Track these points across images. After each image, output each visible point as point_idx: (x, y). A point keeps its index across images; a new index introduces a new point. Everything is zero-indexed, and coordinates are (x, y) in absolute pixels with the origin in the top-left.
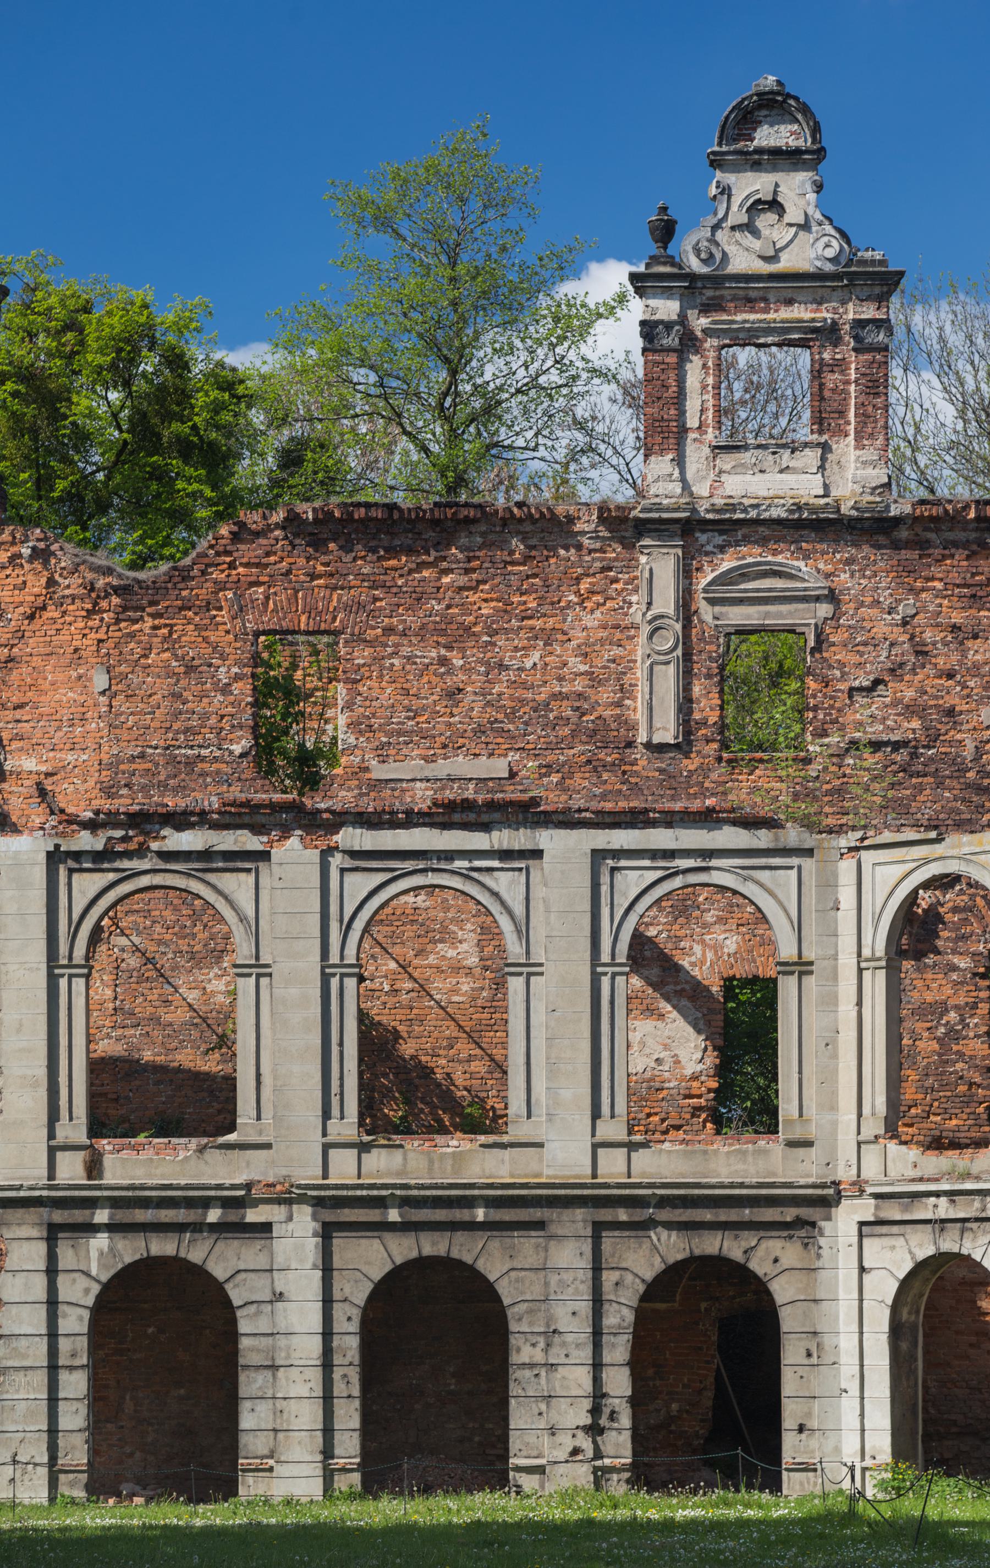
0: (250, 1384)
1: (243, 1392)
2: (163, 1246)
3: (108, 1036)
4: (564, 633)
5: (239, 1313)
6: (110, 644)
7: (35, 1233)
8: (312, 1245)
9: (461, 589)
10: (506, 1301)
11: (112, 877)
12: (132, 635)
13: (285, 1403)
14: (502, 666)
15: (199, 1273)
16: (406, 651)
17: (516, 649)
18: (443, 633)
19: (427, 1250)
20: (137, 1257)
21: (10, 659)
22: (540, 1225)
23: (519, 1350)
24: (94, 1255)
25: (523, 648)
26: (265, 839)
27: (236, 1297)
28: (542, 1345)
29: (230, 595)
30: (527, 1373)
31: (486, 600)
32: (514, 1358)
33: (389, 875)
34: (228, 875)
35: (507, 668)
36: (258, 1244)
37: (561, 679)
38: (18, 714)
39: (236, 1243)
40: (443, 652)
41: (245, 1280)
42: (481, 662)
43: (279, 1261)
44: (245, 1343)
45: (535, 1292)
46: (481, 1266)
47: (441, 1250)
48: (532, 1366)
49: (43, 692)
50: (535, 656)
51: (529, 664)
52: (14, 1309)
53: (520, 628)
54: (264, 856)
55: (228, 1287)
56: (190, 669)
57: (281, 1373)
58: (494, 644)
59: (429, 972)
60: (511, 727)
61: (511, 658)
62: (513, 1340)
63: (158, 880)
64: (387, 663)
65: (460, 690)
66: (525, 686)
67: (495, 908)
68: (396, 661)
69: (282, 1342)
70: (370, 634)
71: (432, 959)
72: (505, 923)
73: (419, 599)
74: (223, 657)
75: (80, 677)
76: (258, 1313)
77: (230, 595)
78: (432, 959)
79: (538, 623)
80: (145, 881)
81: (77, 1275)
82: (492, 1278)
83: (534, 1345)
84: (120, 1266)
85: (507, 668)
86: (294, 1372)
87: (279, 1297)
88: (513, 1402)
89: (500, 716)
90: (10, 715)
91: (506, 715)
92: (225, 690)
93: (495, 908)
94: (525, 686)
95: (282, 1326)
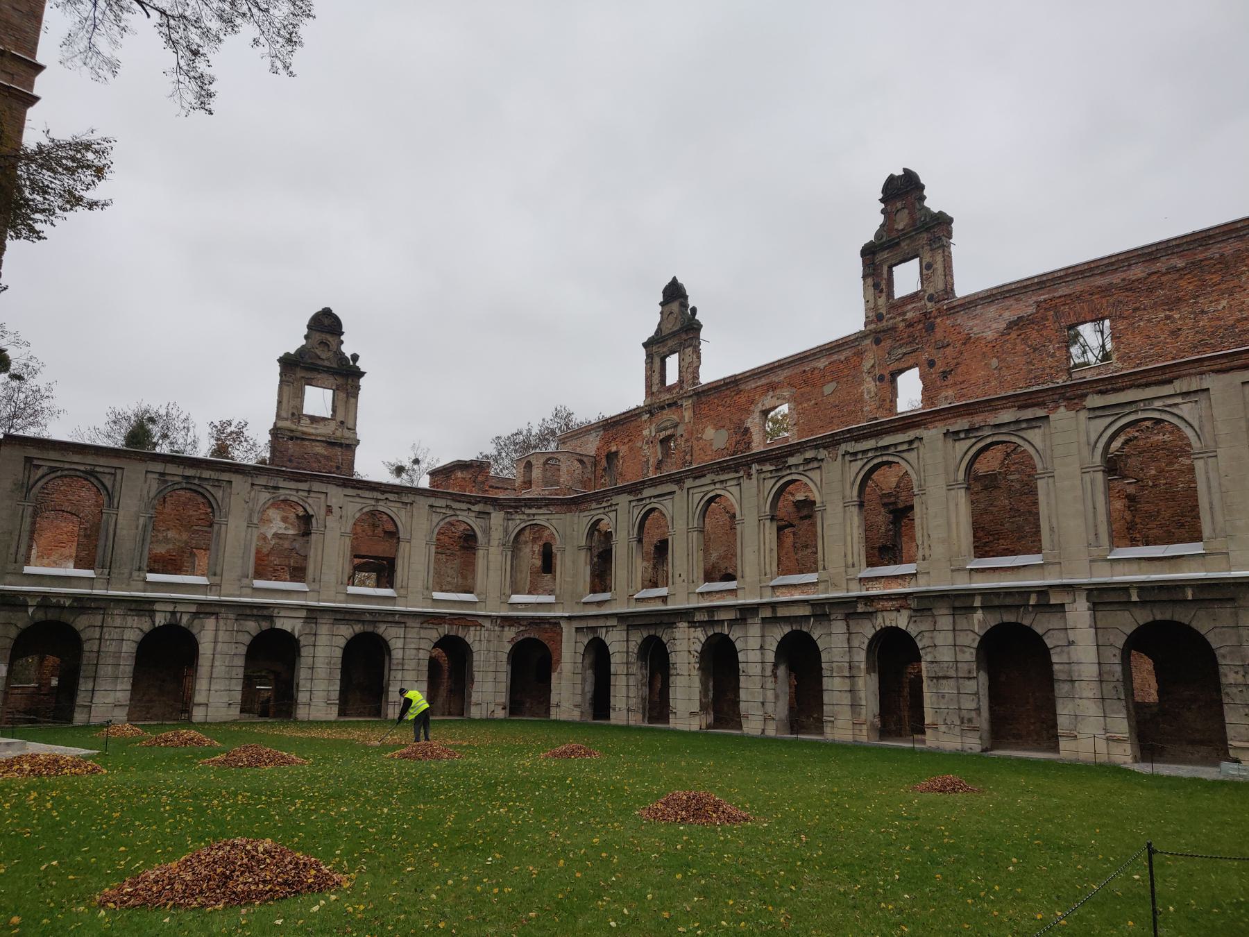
0: (1061, 689)
1: (1057, 693)
2: (1009, 618)
3: (1008, 522)
4: (1241, 287)
5: (1052, 652)
6: (998, 347)
7: (947, 612)
8: (1087, 614)
9: (1175, 280)
10: (1214, 646)
11: (974, 440)
12: (1007, 340)
13: (1080, 701)
14: (1203, 312)
15: (1029, 631)
16: (1146, 317)
17: (1211, 302)
18: (1167, 304)
19: (1159, 617)
20: (997, 623)
21: (958, 364)
22: (1232, 600)
23: (1226, 676)
24: (976, 622)
25: (1216, 301)
26: (1046, 410)
27: (1049, 643)
28: (1242, 673)
29: (1052, 313)
30: (1235, 690)
31: (1189, 283)
32: (1223, 680)
33: (1116, 417)
34: (1029, 431)
35: (1206, 313)
36: (1059, 615)
37: (1240, 311)
38: (962, 386)
39: (1047, 615)
40: (1167, 313)
41: (1053, 634)
42: (1191, 313)
43: (1070, 624)
44: (1056, 667)
45: (1234, 641)
46: (1194, 625)
47: (1168, 616)
48: (1236, 685)
49: (970, 374)
50: (1224, 303)
51: (1220, 308)
52: (940, 649)
53: (1213, 291)
54: (1047, 417)
55: (1045, 638)
56: (1035, 350)
57: (1077, 684)
58: (1198, 303)
59: (1174, 473)
60: (1212, 341)
61: (1208, 307)
62: (1222, 670)
63: (995, 439)
64: (1136, 325)
65: (1180, 330)
66: (1219, 319)
67: (1182, 425)
68: (1141, 323)
69: (1075, 667)
70: (1126, 314)
71: (1176, 466)
72: (1189, 432)
73: (1151, 291)
74: (1050, 341)
75: (986, 364)
76: (1062, 651)
77: (1052, 313)
78: (1176, 466)
79: (1223, 286)
80: (989, 440)
81: (969, 632)
82: (1203, 632)
83: (1237, 673)
84: (989, 627)
85: (1206, 313)
86: (1084, 684)
87: (1071, 643)
88: (1226, 707)
89: (1206, 337)
90: (959, 387)
91: (1208, 336)
92: (1053, 356)
93: (1182, 425)
94: (1219, 319)
95: (1074, 659)
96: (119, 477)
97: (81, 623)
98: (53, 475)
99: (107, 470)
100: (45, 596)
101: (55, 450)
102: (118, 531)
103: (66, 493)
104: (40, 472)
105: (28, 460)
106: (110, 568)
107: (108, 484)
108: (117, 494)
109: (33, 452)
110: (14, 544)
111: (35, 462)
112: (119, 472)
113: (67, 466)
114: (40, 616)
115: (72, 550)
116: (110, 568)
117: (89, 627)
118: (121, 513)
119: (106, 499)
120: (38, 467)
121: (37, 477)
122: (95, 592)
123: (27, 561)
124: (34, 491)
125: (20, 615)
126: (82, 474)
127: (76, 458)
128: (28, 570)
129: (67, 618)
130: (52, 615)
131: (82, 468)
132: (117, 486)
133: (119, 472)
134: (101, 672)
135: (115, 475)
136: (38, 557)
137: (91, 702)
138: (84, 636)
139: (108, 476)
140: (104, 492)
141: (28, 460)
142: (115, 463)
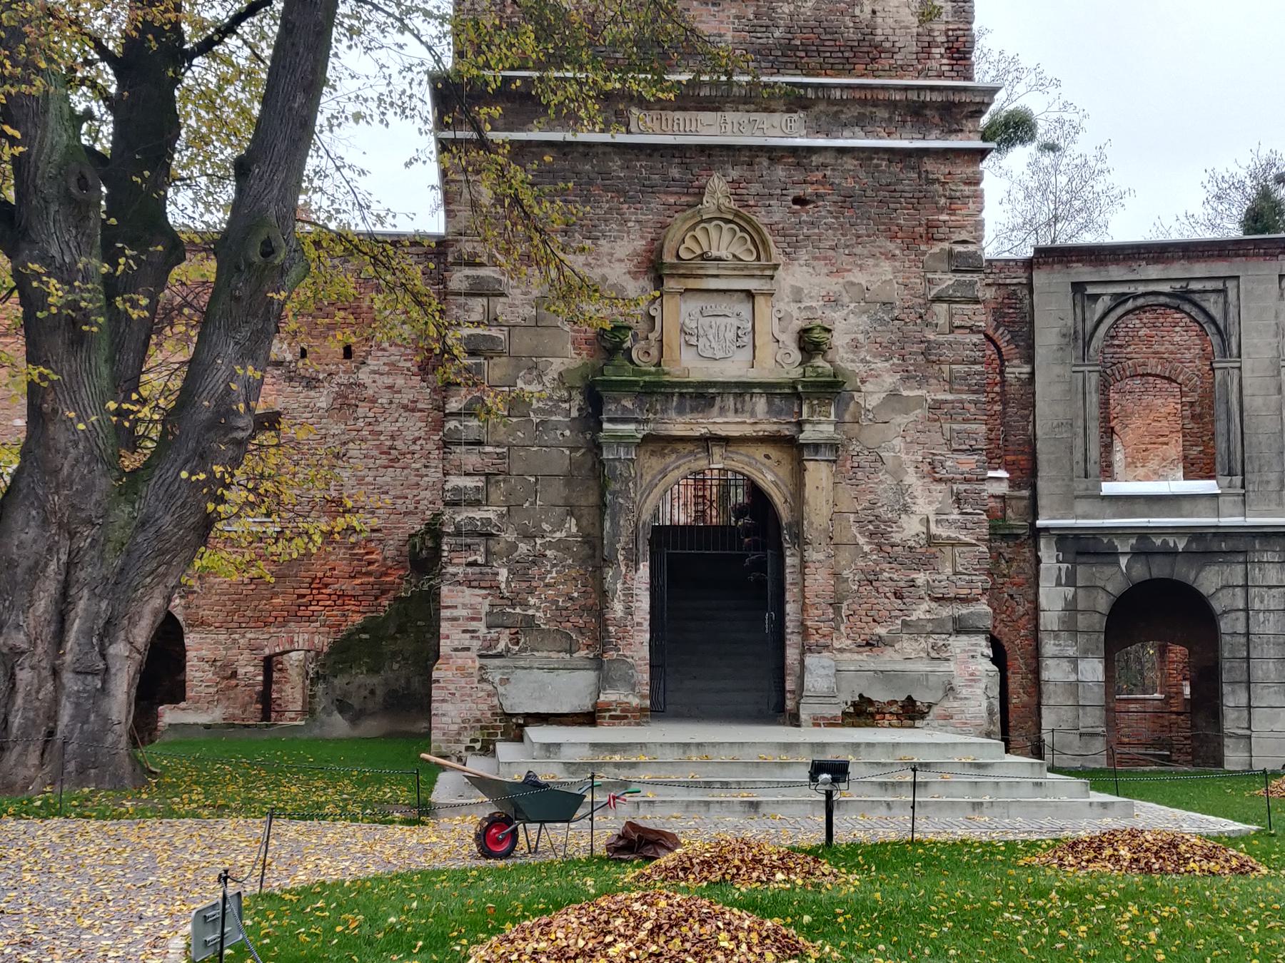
96: (1232, 295)
97: (1209, 580)
98: (1120, 311)
99: (1209, 285)
100: (1143, 534)
101: (1116, 262)
102: (1246, 400)
103: (1148, 341)
104: (1100, 307)
105: (1078, 287)
106: (1243, 474)
107: (1216, 312)
108: (1234, 330)
109: (1083, 272)
110: (1079, 442)
111: (1091, 290)
112: (1231, 285)
113: (1141, 289)
114: (1140, 572)
115: (1174, 449)
116: (1243, 474)
117: (1223, 587)
118: (1247, 364)
119: (1215, 340)
120: (1095, 298)
121: (1096, 317)
122: (1225, 521)
123: (1107, 472)
124: (1094, 343)
125: (1109, 571)
126: (1167, 300)
127: (1153, 271)
128: (1108, 488)
129: (1184, 572)
130: (1160, 569)
131: (1166, 288)
132: (1232, 311)
133: (1231, 285)
134: (1258, 673)
135: (1224, 291)
136: (1128, 465)
137: (1249, 728)
138: (1218, 606)
139: (1213, 297)
140: (1210, 329)
141: (1078, 287)
142: (1221, 268)
